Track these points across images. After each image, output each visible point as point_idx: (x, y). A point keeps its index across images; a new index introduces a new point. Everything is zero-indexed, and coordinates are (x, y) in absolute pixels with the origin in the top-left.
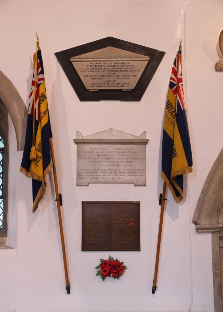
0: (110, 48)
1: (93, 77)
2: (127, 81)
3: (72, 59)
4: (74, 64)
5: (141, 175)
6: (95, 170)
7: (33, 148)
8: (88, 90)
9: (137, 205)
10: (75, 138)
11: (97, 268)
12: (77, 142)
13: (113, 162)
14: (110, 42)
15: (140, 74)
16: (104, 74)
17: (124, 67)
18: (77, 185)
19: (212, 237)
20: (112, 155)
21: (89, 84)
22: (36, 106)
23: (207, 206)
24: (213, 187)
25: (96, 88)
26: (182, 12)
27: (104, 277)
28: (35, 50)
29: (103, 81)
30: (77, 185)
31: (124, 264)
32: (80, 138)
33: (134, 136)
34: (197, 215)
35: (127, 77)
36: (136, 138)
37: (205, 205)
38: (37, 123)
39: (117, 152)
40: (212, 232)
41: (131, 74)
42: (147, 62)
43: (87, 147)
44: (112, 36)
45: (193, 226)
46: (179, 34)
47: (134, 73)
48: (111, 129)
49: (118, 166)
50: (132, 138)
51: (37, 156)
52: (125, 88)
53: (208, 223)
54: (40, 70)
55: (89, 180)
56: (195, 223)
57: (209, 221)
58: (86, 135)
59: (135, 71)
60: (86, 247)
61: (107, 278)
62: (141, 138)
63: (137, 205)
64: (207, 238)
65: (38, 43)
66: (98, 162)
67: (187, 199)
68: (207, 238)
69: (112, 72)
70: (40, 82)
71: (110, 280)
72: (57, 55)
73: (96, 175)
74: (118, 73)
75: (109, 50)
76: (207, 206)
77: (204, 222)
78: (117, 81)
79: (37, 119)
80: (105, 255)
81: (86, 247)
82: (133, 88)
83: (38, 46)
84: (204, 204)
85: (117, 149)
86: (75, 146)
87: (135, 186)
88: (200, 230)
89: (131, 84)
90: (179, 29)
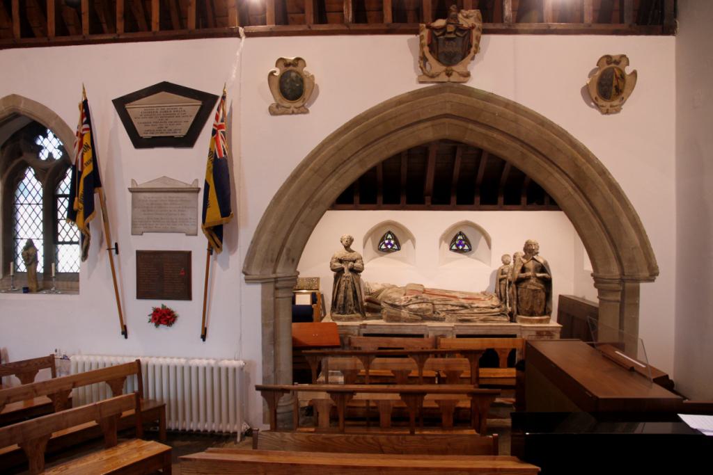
0: (163, 93)
1: (146, 124)
2: (179, 127)
3: (127, 106)
4: (128, 110)
5: (192, 225)
6: (148, 219)
7: (76, 199)
8: (142, 138)
9: (140, 254)
10: (130, 187)
11: (149, 315)
12: (132, 190)
13: (165, 211)
14: (165, 87)
15: (192, 120)
16: (156, 120)
17: (176, 113)
18: (132, 234)
19: (262, 287)
20: (165, 204)
21: (143, 132)
22: (79, 157)
23: (258, 256)
24: (264, 238)
25: (149, 135)
26: (238, 54)
27: (157, 325)
28: (80, 100)
29: (155, 128)
30: (132, 234)
31: (152, 312)
32: (135, 186)
33: (187, 184)
34: (246, 266)
35: (179, 123)
36: (188, 187)
37: (256, 255)
38: (81, 173)
39: (169, 201)
40: (262, 283)
41: (184, 119)
42: (199, 107)
43: (142, 196)
44: (166, 81)
45: (243, 276)
46: (234, 76)
47: (186, 119)
48: (164, 177)
49: (170, 215)
50: (184, 186)
51: (79, 207)
52: (177, 135)
53: (259, 274)
54: (85, 119)
55: (142, 229)
56: (245, 274)
57: (260, 272)
58: (141, 182)
59: (187, 116)
60: (141, 295)
61: (161, 326)
62: (193, 187)
63: (140, 254)
64: (257, 288)
65: (84, 93)
66: (151, 211)
67: (238, 250)
68: (257, 288)
69: (164, 118)
70: (84, 133)
71: (163, 328)
72: (114, 101)
73: (150, 224)
74: (171, 119)
75: (163, 95)
76: (258, 256)
77: (255, 273)
78: (170, 127)
79: (80, 169)
80: (158, 304)
81: (141, 295)
82: (184, 134)
83: (85, 96)
84: (255, 254)
85: (170, 197)
86: (130, 195)
87: (187, 235)
88: (249, 280)
89: (182, 130)
90: (234, 71)
